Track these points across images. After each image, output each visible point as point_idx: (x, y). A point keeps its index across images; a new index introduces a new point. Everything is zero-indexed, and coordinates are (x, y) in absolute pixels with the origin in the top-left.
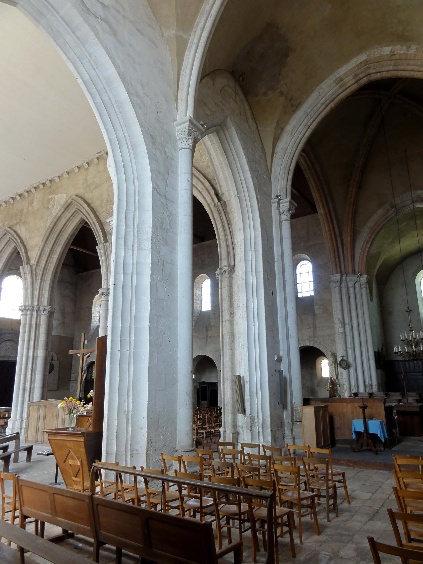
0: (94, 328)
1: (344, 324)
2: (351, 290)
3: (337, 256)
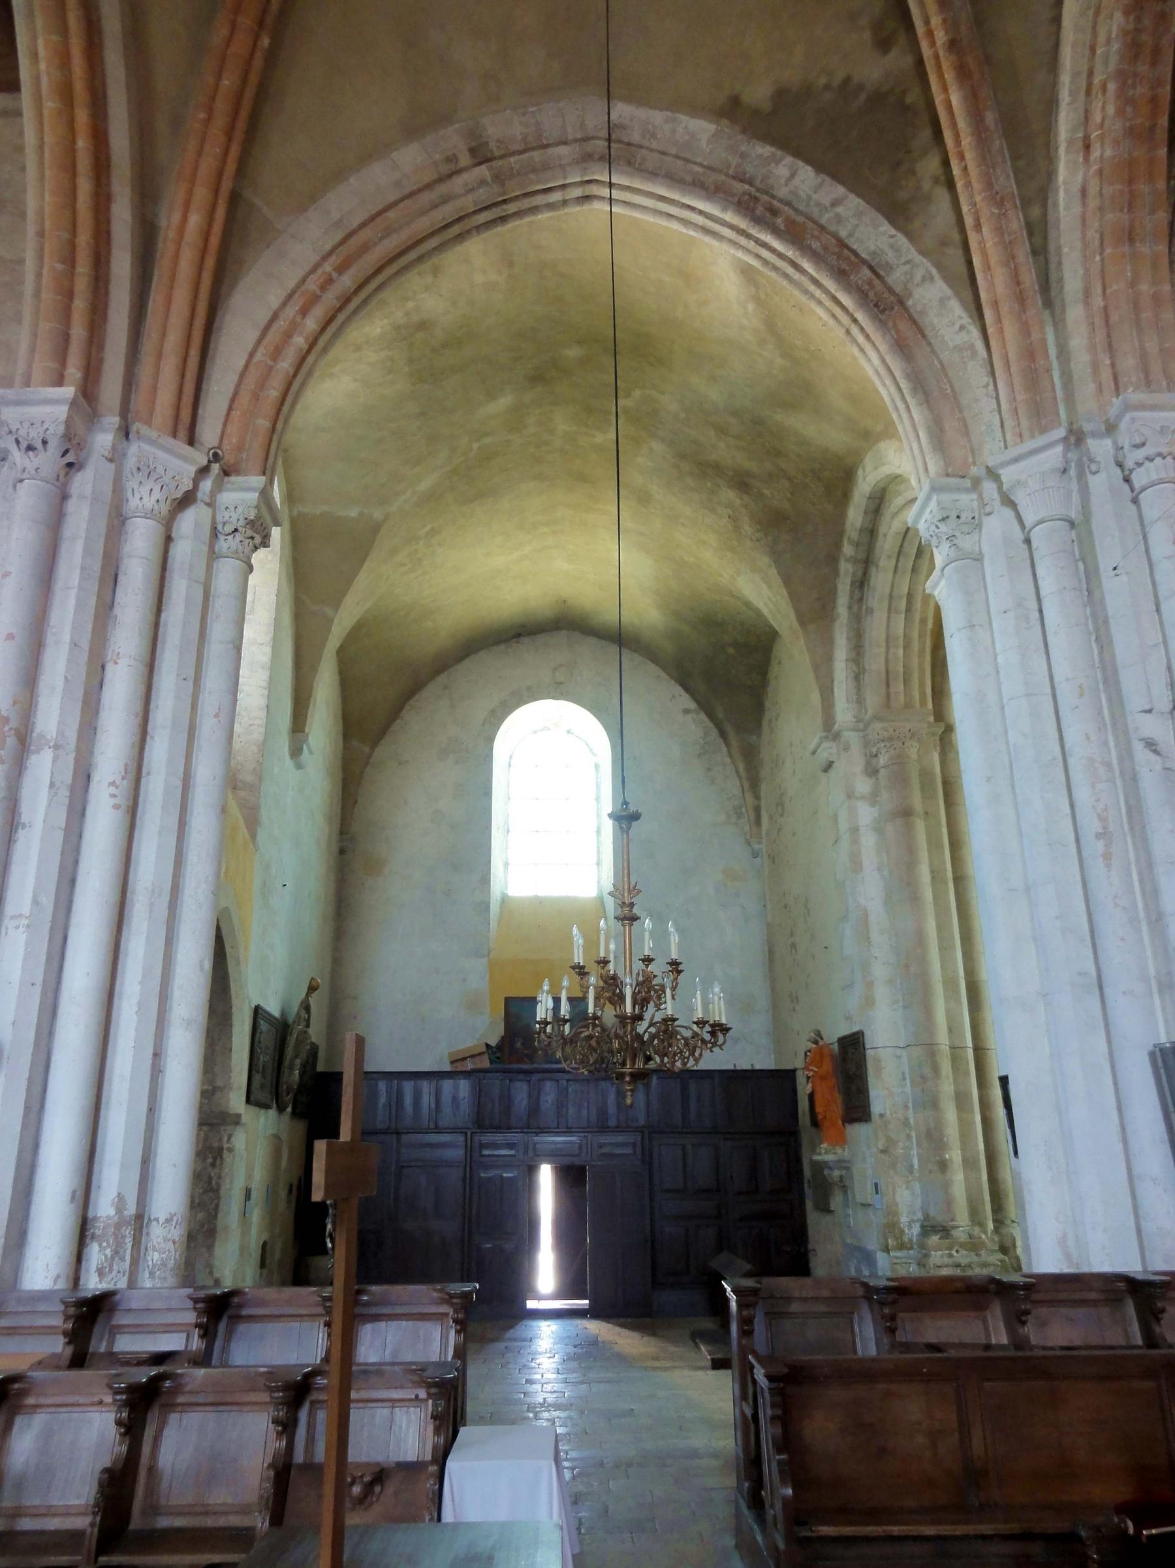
3: (82, 284)
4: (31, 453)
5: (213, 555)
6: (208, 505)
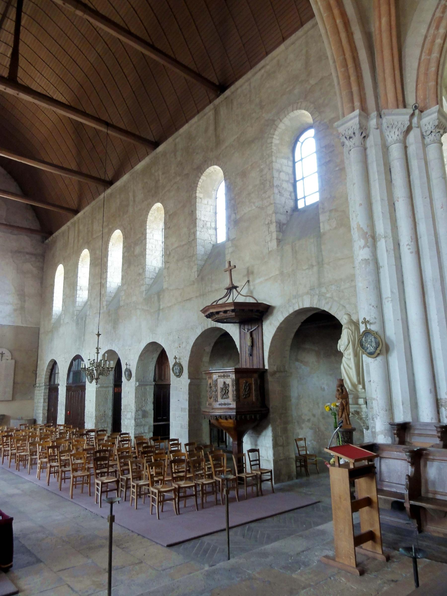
0: (57, 313)
1: (372, 239)
2: (395, 152)
4: (351, 139)
5: (425, 146)
6: (418, 127)
